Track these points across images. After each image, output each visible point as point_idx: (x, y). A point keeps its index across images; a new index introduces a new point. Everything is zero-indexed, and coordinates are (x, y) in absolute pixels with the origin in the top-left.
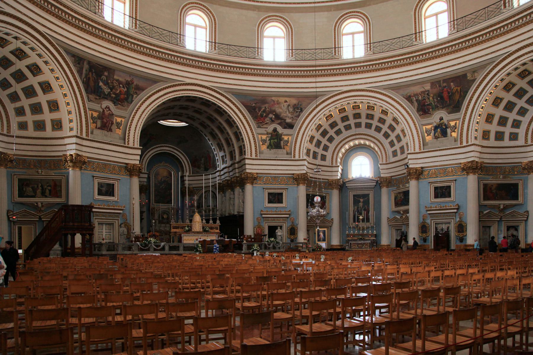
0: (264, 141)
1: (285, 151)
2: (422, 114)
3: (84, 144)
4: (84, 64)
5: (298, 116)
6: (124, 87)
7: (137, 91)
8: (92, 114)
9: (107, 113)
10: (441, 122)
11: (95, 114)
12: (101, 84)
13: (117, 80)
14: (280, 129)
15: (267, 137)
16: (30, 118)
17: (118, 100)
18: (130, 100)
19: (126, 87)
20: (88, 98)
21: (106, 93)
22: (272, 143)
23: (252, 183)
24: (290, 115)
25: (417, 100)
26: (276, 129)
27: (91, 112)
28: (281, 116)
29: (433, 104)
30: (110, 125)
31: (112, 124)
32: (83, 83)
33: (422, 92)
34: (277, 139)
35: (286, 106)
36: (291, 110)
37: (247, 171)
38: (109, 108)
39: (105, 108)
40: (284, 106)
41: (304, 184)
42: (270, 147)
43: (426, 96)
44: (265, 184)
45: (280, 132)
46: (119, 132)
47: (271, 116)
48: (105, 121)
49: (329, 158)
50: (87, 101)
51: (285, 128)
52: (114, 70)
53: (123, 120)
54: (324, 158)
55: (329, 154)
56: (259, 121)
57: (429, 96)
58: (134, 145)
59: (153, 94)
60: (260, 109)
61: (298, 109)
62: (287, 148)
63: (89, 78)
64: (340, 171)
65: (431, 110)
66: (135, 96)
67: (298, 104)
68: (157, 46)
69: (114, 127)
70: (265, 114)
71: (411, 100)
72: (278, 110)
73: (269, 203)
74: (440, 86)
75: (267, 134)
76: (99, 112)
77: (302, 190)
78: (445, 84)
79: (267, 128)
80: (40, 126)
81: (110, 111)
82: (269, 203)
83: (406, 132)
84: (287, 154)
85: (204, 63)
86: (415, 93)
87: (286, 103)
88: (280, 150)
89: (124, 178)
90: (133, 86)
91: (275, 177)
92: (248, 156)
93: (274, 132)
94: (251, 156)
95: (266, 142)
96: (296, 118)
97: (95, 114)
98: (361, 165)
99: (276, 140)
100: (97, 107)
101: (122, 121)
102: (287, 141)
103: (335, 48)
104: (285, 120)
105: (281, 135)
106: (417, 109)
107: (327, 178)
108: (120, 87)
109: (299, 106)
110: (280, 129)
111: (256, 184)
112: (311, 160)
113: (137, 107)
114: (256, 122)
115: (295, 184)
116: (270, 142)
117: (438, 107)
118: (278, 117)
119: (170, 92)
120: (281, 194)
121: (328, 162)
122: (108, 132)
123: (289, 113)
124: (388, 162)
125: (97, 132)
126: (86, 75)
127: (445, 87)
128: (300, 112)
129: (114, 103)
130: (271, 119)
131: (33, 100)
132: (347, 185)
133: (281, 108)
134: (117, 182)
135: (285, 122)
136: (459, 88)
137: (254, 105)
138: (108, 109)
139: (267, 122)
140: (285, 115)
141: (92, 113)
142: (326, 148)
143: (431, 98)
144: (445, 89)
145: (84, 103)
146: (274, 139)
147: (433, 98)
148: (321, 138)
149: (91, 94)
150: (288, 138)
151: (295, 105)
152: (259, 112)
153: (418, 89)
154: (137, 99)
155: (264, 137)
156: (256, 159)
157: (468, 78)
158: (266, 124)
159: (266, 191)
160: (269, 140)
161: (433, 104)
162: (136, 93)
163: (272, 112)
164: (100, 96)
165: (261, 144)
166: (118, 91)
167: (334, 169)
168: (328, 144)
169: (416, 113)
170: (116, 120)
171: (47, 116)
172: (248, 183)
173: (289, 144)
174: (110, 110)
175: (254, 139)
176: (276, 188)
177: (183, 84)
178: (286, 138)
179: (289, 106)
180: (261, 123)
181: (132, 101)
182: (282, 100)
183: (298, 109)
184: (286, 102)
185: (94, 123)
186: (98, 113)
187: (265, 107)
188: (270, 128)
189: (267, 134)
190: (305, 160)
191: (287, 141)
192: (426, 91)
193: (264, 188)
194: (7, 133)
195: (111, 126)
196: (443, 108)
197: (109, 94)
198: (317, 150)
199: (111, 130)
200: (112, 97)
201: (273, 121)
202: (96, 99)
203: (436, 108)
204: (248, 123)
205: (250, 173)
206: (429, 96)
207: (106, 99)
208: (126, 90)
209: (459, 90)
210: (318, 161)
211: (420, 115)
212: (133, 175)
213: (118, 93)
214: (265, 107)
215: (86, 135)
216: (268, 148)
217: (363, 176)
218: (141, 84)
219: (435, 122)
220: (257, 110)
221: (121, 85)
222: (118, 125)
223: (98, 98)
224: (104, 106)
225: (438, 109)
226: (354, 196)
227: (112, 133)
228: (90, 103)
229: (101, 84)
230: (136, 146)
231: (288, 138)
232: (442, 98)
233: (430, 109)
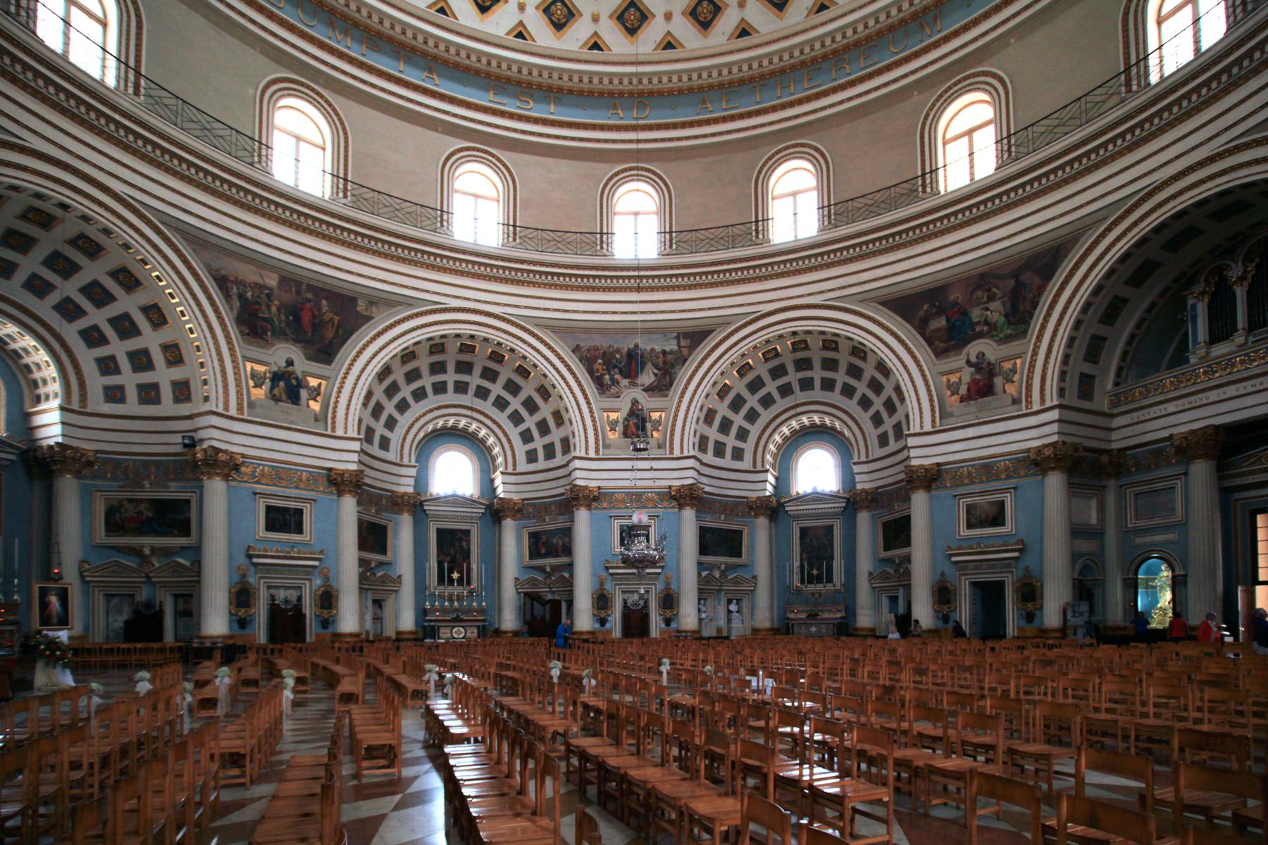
3: (235, 429)
49: (748, 456)
54: (738, 454)
55: (748, 447)
64: (771, 479)
80: (149, 393)
83: (904, 389)
84: (660, 446)
92: (580, 452)
124: (871, 458)
132: (787, 509)
142: (743, 435)
150: (660, 416)
167: (760, 477)
168: (746, 425)
171: (164, 375)
190: (693, 457)
191: (659, 422)
215: (238, 409)
217: (819, 490)
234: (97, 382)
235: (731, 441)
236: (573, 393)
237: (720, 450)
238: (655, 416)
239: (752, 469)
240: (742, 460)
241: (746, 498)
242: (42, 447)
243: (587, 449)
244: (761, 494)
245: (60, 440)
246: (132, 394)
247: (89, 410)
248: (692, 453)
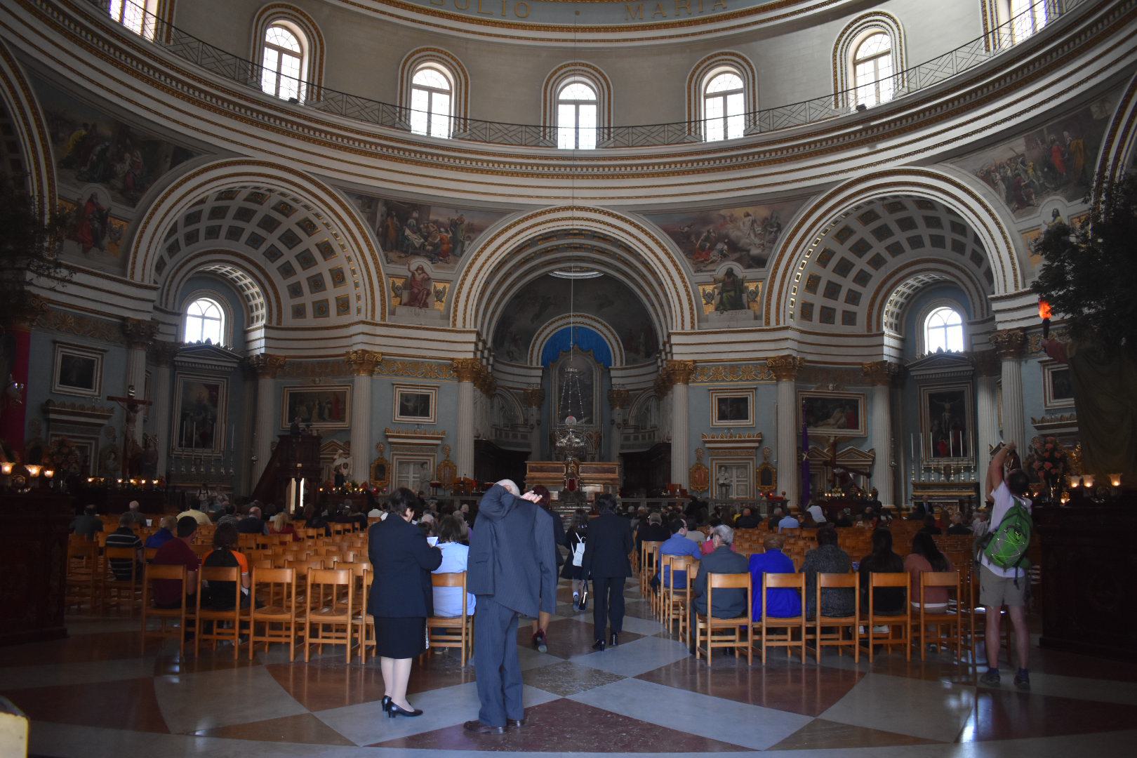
0: (709, 297)
1: (750, 313)
2: (1018, 208)
4: (377, 206)
5: (774, 241)
6: (447, 231)
7: (472, 235)
8: (394, 283)
9: (419, 277)
10: (1056, 221)
11: (399, 283)
12: (408, 232)
13: (435, 222)
14: (739, 271)
15: (715, 288)
16: (308, 298)
17: (437, 255)
18: (458, 251)
19: (452, 231)
21: (417, 246)
22: (724, 300)
23: (686, 382)
24: (757, 241)
25: (1004, 179)
26: (732, 270)
27: (391, 281)
28: (740, 245)
29: (1036, 183)
31: (428, 294)
32: (377, 235)
33: (1010, 159)
34: (736, 292)
35: (748, 224)
36: (759, 229)
37: (676, 358)
38: (422, 269)
39: (417, 270)
40: (744, 223)
41: (789, 377)
42: (721, 307)
43: (1020, 166)
44: (711, 381)
45: (740, 276)
46: (440, 306)
47: (720, 246)
48: (416, 291)
49: (861, 319)
50: (385, 262)
51: (749, 267)
52: (430, 206)
53: (448, 285)
54: (849, 318)
55: (861, 310)
56: (697, 258)
57: (1025, 165)
58: (464, 327)
59: (498, 235)
60: (698, 235)
61: (772, 227)
62: (755, 306)
63: (388, 226)
65: (1033, 197)
66: (467, 243)
67: (772, 217)
68: (500, 155)
69: (432, 299)
70: (708, 245)
71: (993, 182)
72: (734, 234)
73: (720, 418)
74: (1043, 141)
75: (716, 281)
76: (406, 277)
77: (786, 392)
78: (1053, 137)
79: (714, 270)
82: (720, 418)
84: (757, 318)
85: (587, 167)
86: (998, 162)
87: (748, 218)
88: (741, 311)
89: (448, 383)
90: (463, 226)
91: (732, 366)
93: (729, 277)
94: (683, 328)
95: (713, 299)
96: (768, 245)
97: (399, 283)
98: (946, 326)
99: (732, 293)
100: (402, 270)
101: (445, 288)
102: (755, 293)
103: (836, 94)
104: (748, 251)
105: (742, 281)
106: (1007, 197)
107: (859, 360)
108: (441, 232)
109: (774, 220)
110: (739, 271)
111: (694, 382)
112: (816, 324)
113: (470, 261)
114: (692, 261)
115: (771, 379)
116: (721, 299)
117: (1046, 188)
118: (734, 247)
119: (528, 228)
120: (745, 400)
121: (860, 326)
123: (756, 236)
124: (986, 317)
125: (402, 311)
126: (383, 223)
127: (1053, 142)
128: (776, 232)
129: (431, 260)
130: (721, 251)
131: (312, 271)
133: (739, 229)
134: (434, 392)
135: (749, 255)
136: (1081, 141)
137: (686, 229)
138: (420, 272)
139: (714, 258)
140: (748, 241)
141: (394, 283)
142: (853, 298)
143: (1030, 171)
144: (1055, 147)
145: (377, 268)
146: (728, 291)
147: (1034, 170)
148: (836, 279)
149: (391, 251)
151: (766, 219)
152: (697, 241)
153: (999, 154)
154: (471, 249)
155: (709, 289)
156: (692, 334)
157: (1095, 117)
158: (712, 262)
159: (714, 395)
160: (719, 293)
161: (1036, 183)
162: (469, 238)
163: (723, 238)
164: (406, 252)
165: (704, 302)
167: (875, 341)
169: (1006, 206)
170: (435, 287)
171: (331, 293)
172: (679, 380)
173: (758, 299)
174: (424, 272)
175: (688, 294)
176: (731, 386)
177: (549, 212)
178: (752, 287)
179: (754, 222)
180: (702, 262)
181: (463, 252)
182: (739, 212)
183: (772, 227)
184: (748, 215)
185: (396, 296)
186: (403, 280)
187: (708, 231)
188: (721, 270)
189: (716, 281)
191: (755, 293)
192: (1018, 156)
193: (710, 390)
194: (278, 324)
195: (426, 298)
196: (1055, 189)
197: (423, 245)
198: (830, 303)
199: (425, 305)
200: (428, 251)
201: (724, 256)
202: (400, 257)
203: (1042, 192)
204: (675, 265)
205: (680, 362)
206: (1025, 165)
207: (418, 254)
208: (450, 235)
209: (1082, 147)
210: (838, 326)
211: (1013, 211)
212: (463, 377)
213: (437, 243)
214: (708, 231)
216: (716, 309)
218: (476, 221)
219: (1044, 222)
220: (693, 238)
221: (442, 230)
222: (439, 295)
223: (403, 255)
224: (413, 267)
225: (1048, 194)
226: (931, 396)
227: (428, 311)
228: (390, 265)
229: (408, 232)
230: (468, 328)
231: (757, 287)
232: (1051, 167)
233: (1032, 194)
234: (288, 303)
235: (840, 305)
236: (669, 273)
237: (827, 316)
238: (752, 287)
239: (866, 333)
240: (854, 324)
241: (861, 364)
242: (252, 356)
243: (683, 325)
244: (878, 359)
245: (263, 351)
246: (309, 310)
247: (283, 326)
248: (790, 322)
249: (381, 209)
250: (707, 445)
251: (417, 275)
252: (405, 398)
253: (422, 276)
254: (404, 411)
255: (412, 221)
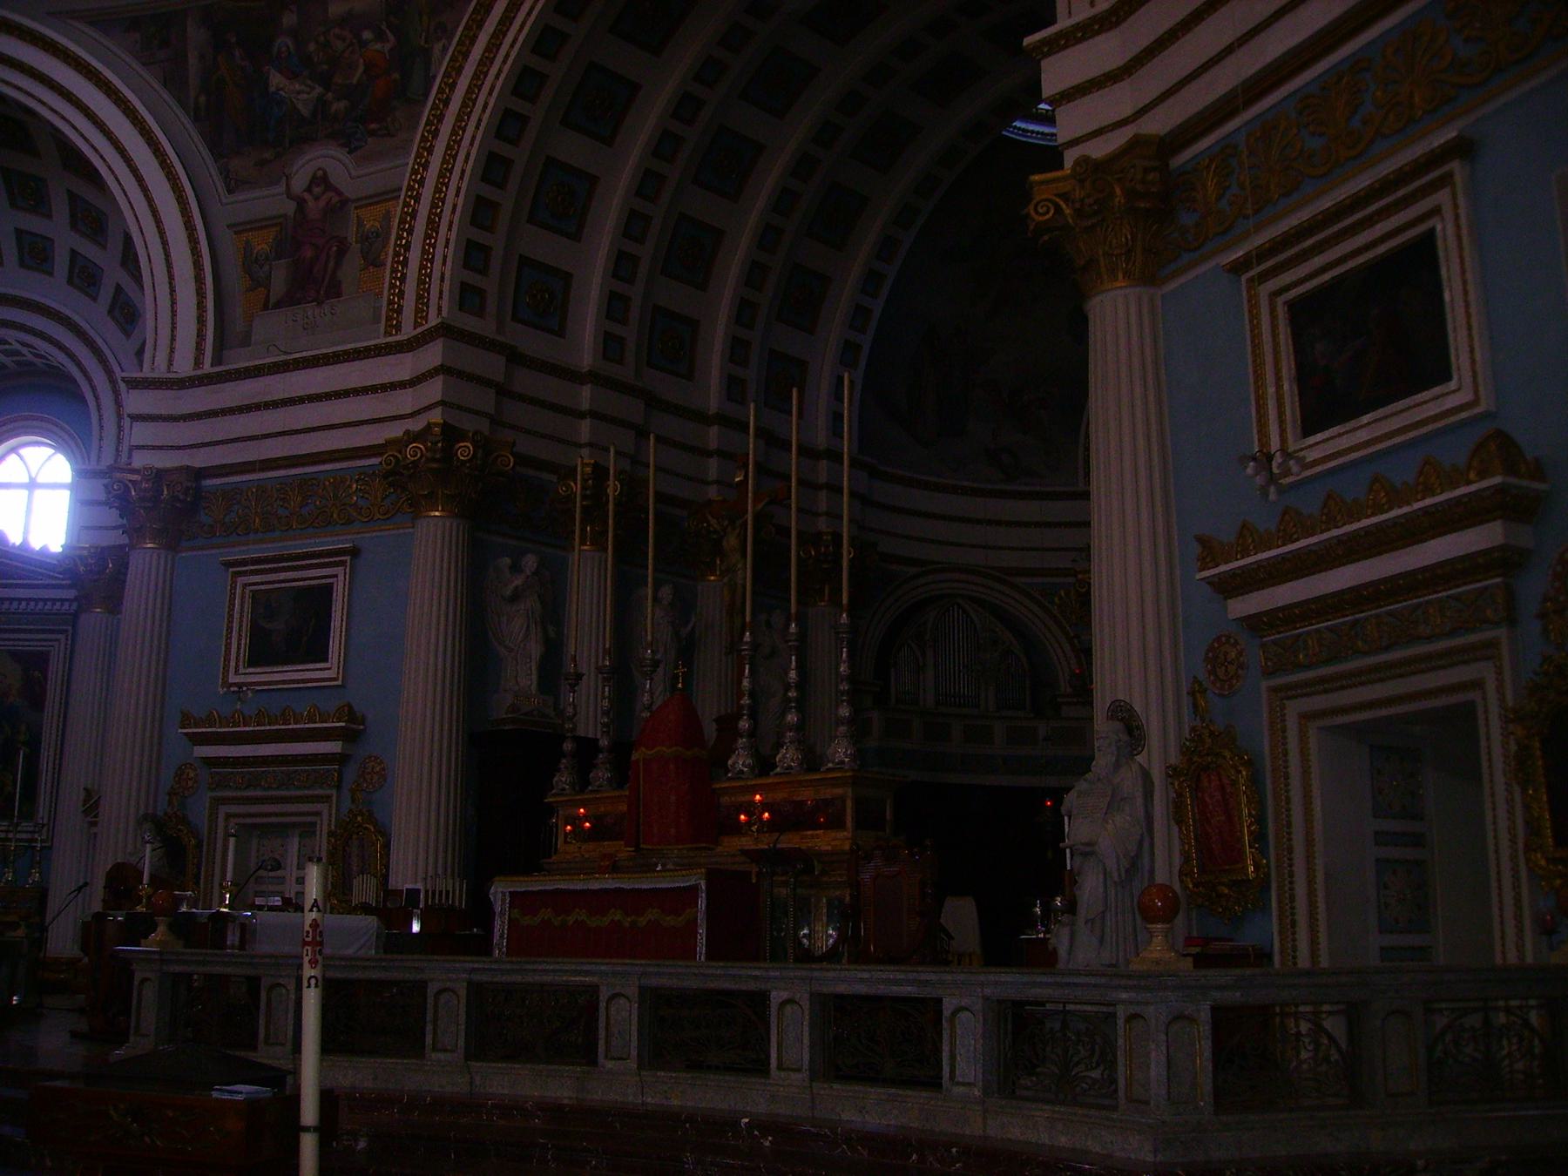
6: (380, 37)
9: (314, 208)
12: (276, 80)
20: (226, 174)
30: (331, 264)
32: (196, 120)
39: (309, 190)
50: (222, 189)
81: (332, 194)
97: (262, 243)
100: (269, 201)
108: (363, 44)
122: (320, 304)
129: (349, 143)
138: (317, 190)
166: (361, 69)
174: (329, 187)
199: (335, 290)
221: (367, 35)
223: (268, 155)
224: (299, 183)
228: (232, 198)
229: (276, 80)
249: (196, 36)
250: (1245, 606)
251: (311, 203)
252: (263, 603)
253: (322, 204)
254: (260, 654)
255: (283, 43)
